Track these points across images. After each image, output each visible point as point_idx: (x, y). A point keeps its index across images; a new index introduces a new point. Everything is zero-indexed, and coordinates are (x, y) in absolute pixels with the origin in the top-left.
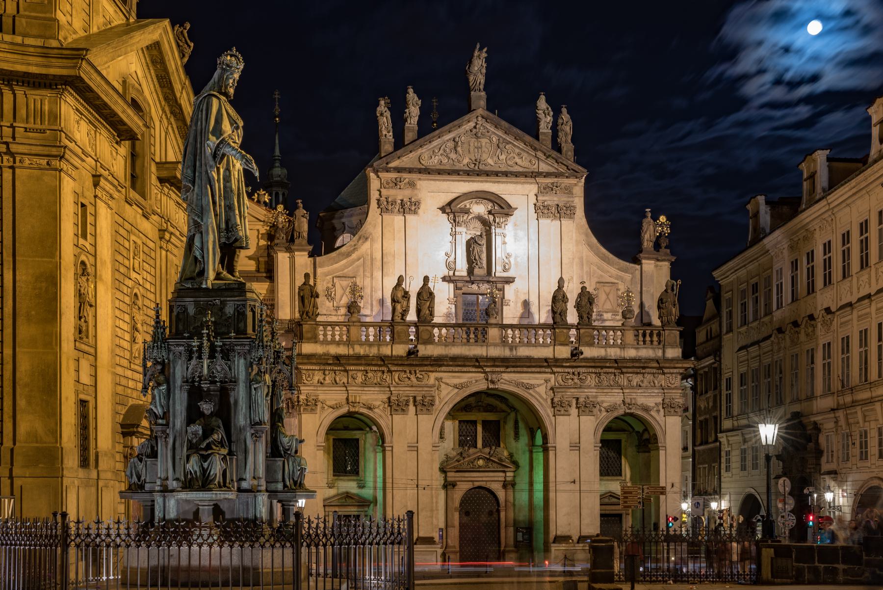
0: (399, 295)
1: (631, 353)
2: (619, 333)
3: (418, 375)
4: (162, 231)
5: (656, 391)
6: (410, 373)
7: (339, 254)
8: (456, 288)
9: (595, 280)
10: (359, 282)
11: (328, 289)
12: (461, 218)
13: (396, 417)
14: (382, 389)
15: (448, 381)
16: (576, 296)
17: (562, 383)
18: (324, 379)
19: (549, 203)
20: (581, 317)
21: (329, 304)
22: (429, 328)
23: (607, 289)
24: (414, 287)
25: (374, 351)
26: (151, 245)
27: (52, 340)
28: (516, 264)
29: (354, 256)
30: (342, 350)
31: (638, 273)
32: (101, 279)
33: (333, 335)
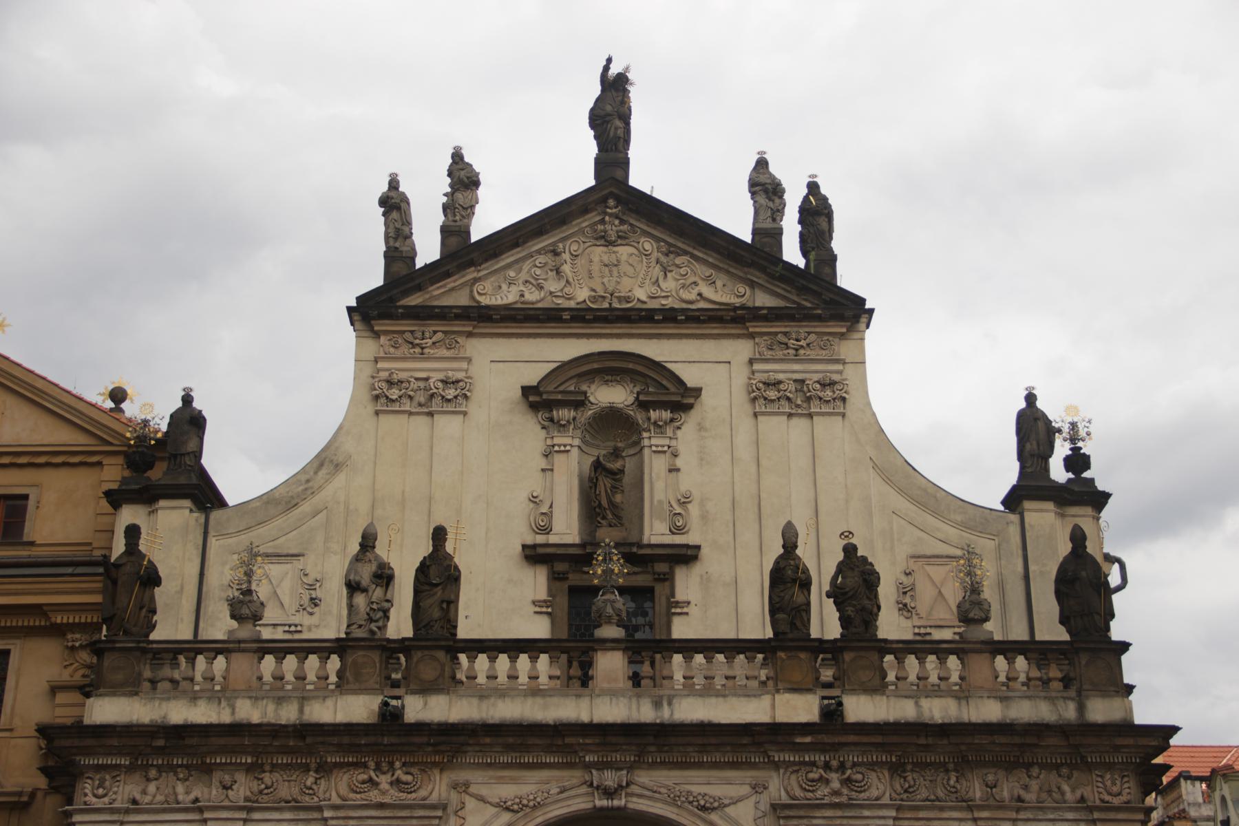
1: (988, 711)
2: (953, 662)
3: (399, 773)
5: (1070, 816)
6: (378, 768)
7: (268, 503)
8: (555, 577)
9: (902, 551)
10: (311, 564)
12: (564, 414)
14: (302, 815)
15: (484, 791)
16: (832, 569)
17: (798, 792)
18: (144, 792)
19: (781, 376)
20: (845, 621)
22: (441, 655)
23: (938, 572)
24: (405, 557)
25: (288, 714)
28: (704, 517)
29: (306, 507)
30: (202, 713)
31: (1014, 532)
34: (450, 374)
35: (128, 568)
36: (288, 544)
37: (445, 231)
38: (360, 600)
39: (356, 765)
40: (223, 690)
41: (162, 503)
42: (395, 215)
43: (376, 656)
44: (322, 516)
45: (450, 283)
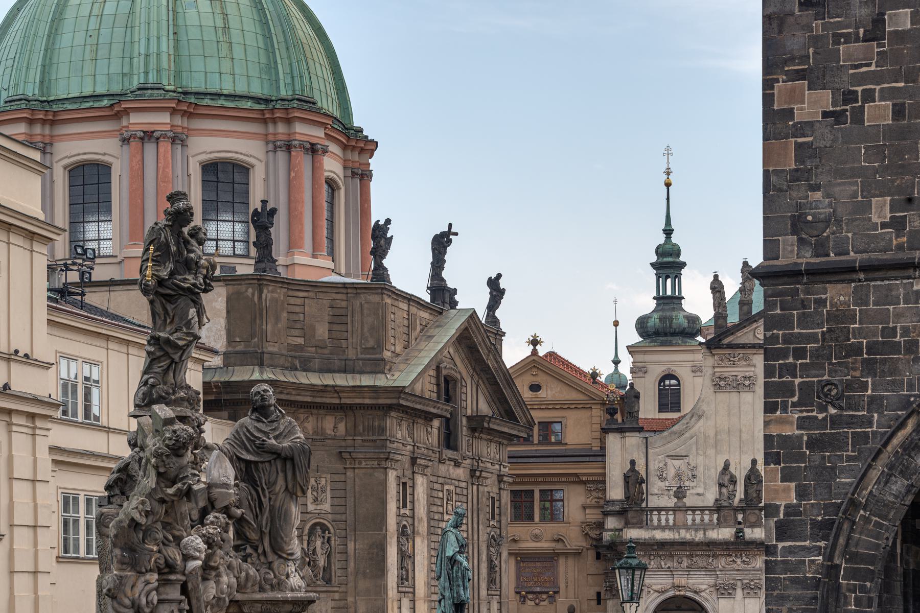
0: (726, 478)
4: (473, 472)
6: (736, 556)
7: (671, 433)
11: (660, 469)
13: (723, 603)
21: (661, 484)
22: (757, 512)
24: (740, 471)
25: (699, 536)
26: (464, 485)
27: (382, 590)
29: (687, 435)
30: (667, 535)
32: (418, 533)
33: (659, 520)
34: (747, 374)
35: (633, 478)
36: (681, 451)
37: (742, 303)
38: (724, 490)
39: (728, 555)
40: (674, 525)
41: (627, 434)
42: (718, 294)
43: (732, 513)
44: (695, 438)
45: (745, 330)
